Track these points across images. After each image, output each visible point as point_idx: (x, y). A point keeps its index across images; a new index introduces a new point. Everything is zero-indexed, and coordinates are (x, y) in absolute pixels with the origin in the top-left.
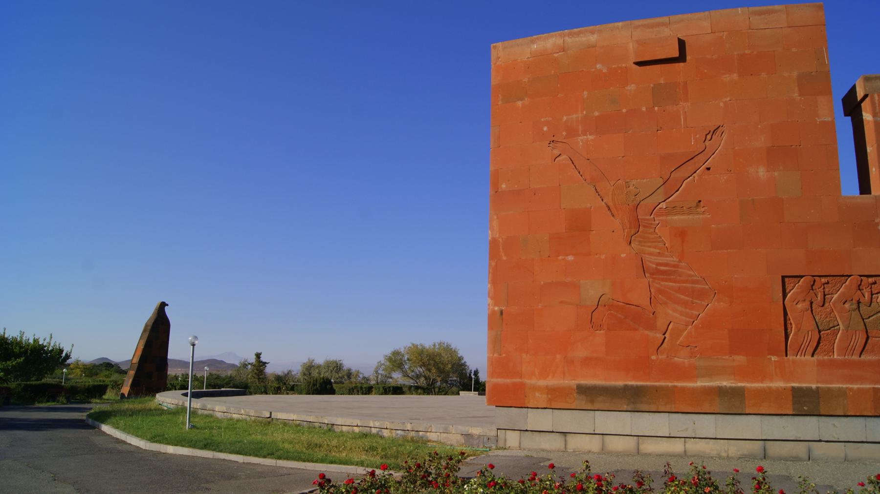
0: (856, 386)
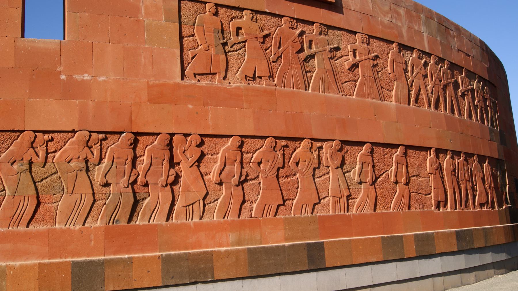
0: (18, 263)
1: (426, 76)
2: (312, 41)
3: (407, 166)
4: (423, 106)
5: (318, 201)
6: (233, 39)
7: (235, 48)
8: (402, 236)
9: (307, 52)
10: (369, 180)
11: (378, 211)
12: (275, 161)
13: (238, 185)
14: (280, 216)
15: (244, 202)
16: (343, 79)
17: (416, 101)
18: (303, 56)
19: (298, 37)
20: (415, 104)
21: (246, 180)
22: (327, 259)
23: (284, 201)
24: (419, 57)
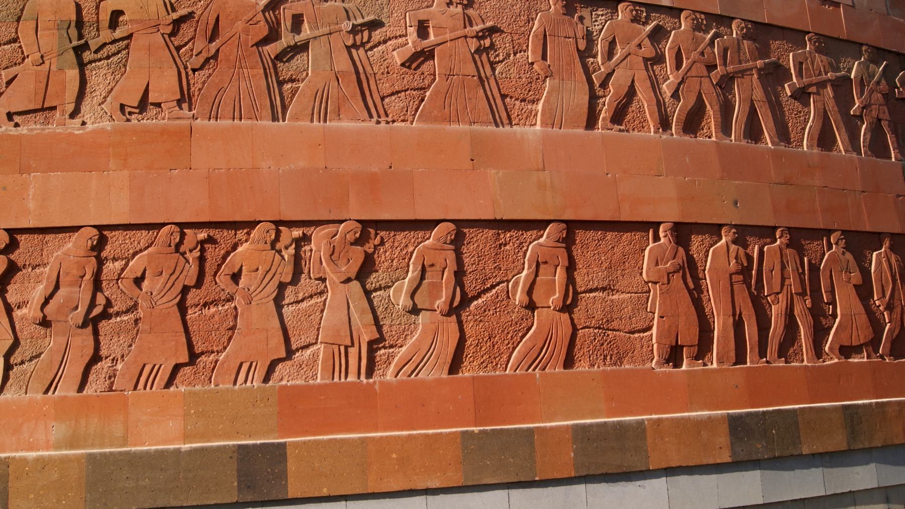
1: (659, 59)
2: (301, 15)
3: (571, 268)
4: (642, 127)
5: (284, 355)
6: (106, 35)
7: (104, 52)
8: (531, 431)
9: (287, 39)
10: (441, 302)
11: (466, 373)
12: (177, 273)
13: (84, 325)
14: (180, 388)
15: (96, 358)
16: (386, 88)
17: (618, 117)
18: (272, 49)
19: (263, 11)
20: (610, 125)
21: (105, 315)
22: (291, 480)
23: (193, 357)
24: (635, 20)
